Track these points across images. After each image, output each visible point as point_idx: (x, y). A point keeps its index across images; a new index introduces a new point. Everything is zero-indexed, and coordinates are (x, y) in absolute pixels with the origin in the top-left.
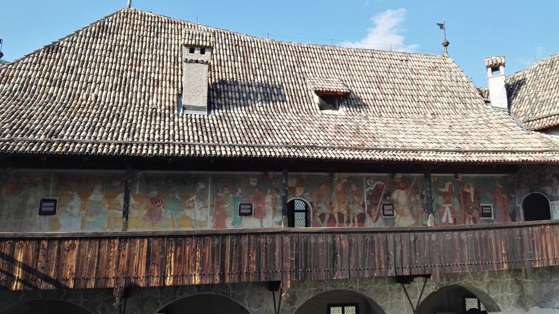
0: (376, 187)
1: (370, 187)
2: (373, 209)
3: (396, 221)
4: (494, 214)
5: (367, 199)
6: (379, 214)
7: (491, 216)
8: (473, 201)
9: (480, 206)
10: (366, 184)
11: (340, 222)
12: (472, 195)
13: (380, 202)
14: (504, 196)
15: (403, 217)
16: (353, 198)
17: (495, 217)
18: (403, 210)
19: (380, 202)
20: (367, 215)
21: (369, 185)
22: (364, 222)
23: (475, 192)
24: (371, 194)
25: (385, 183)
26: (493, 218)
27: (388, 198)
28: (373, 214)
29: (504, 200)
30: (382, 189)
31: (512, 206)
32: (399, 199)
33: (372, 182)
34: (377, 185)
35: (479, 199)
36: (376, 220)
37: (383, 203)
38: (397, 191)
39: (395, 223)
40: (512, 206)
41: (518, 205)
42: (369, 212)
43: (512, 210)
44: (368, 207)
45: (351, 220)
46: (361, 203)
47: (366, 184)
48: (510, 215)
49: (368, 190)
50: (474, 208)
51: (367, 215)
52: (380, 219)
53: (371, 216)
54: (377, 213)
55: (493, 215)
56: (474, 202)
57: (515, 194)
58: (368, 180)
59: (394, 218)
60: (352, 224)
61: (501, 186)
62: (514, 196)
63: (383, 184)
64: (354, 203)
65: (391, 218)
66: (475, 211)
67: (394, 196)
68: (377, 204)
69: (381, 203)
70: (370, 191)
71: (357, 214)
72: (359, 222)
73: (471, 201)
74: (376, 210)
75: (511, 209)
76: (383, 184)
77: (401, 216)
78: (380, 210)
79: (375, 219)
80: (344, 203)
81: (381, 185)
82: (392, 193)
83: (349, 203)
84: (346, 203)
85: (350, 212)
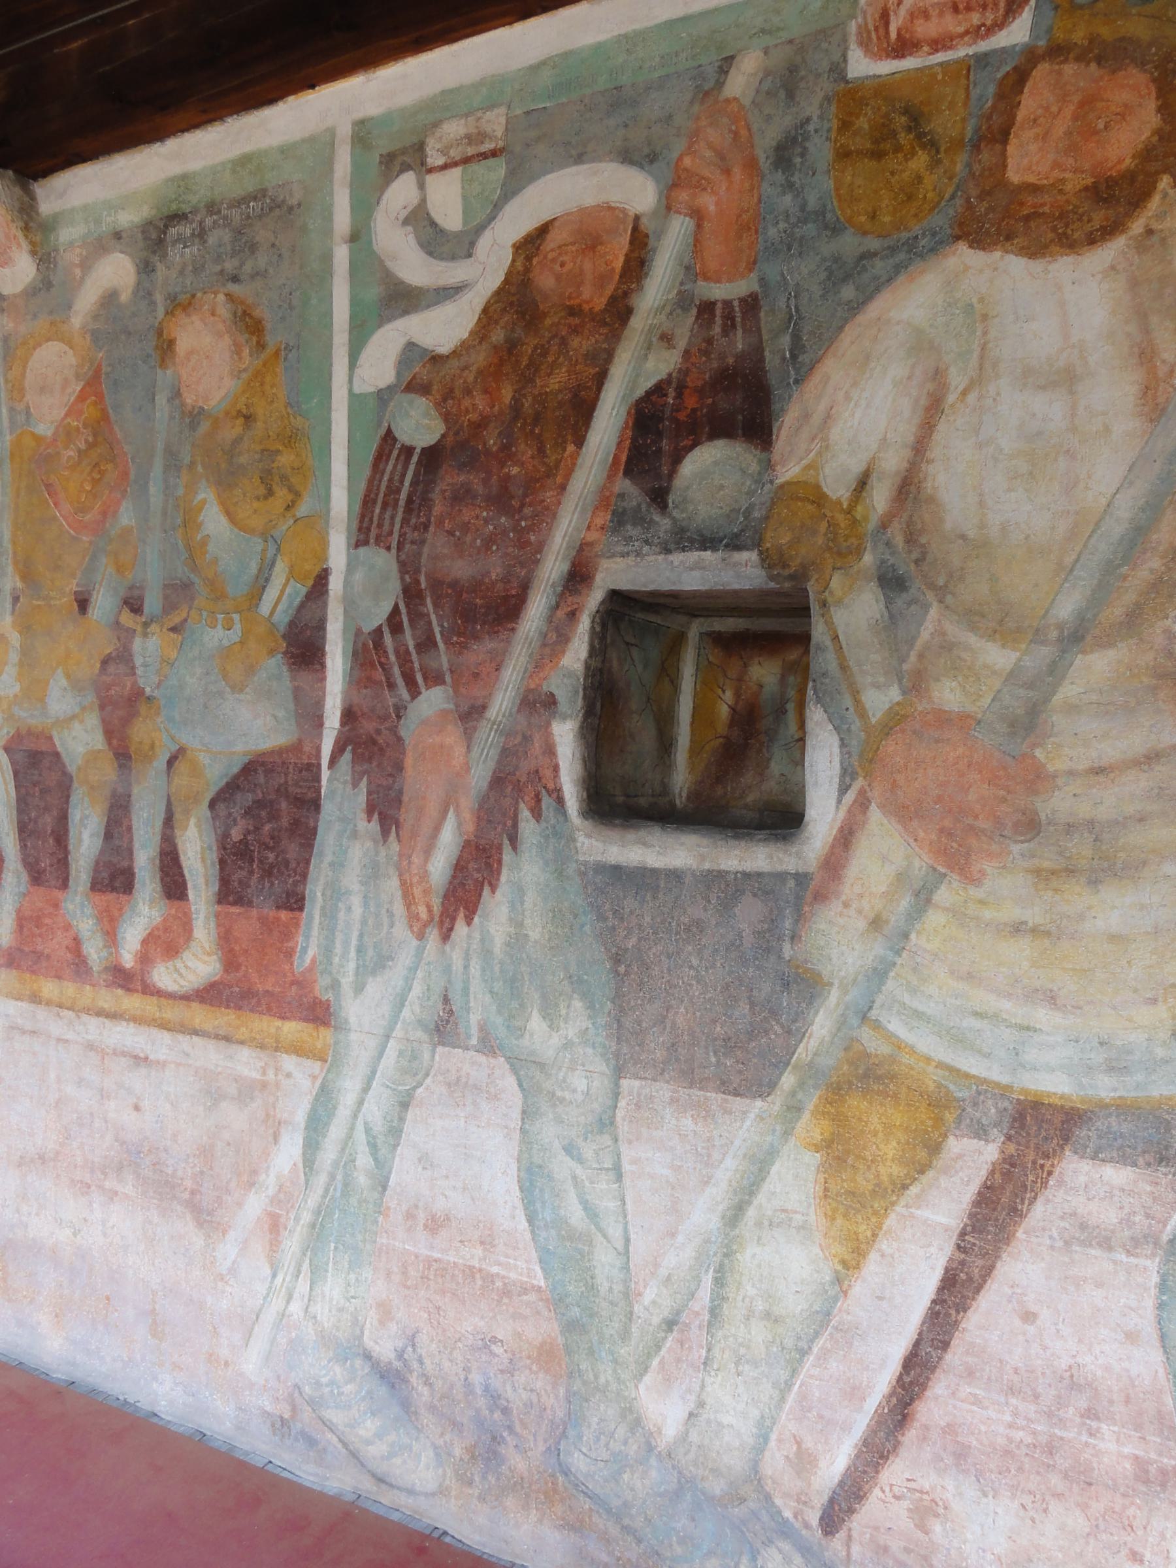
0: (516, 301)
1: (402, 299)
2: (433, 701)
3: (839, 942)
5: (365, 533)
6: (516, 786)
10: (366, 260)
11: (37, 877)
13: (553, 567)
15: (1006, 888)
16: (190, 520)
18: (1028, 722)
19: (553, 567)
20: (341, 796)
21: (414, 267)
22: (295, 902)
24: (420, 426)
25: (676, 185)
27: (710, 472)
28: (421, 782)
30: (619, 312)
32: (953, 482)
33: (447, 198)
34: (531, 246)
36: (465, 892)
37: (619, 572)
38: (914, 303)
39: (804, 984)
42: (372, 743)
44: (367, 654)
45: (144, 858)
46: (280, 598)
47: (366, 260)
49: (379, 365)
51: (341, 796)
52: (525, 872)
53: (386, 810)
54: (480, 775)
58: (402, 192)
59: (810, 891)
60: (145, 912)
63: (637, 192)
64: (184, 594)
65: (729, 889)
67: (850, 417)
68: (506, 609)
69: (578, 576)
70: (423, 374)
71: (216, 772)
72: (229, 893)
74: (470, 714)
76: (637, 192)
77: (956, 848)
78: (537, 704)
79: (439, 866)
80: (83, 604)
81: (590, 229)
82: (801, 363)
83: (134, 605)
84: (103, 604)
85: (140, 732)
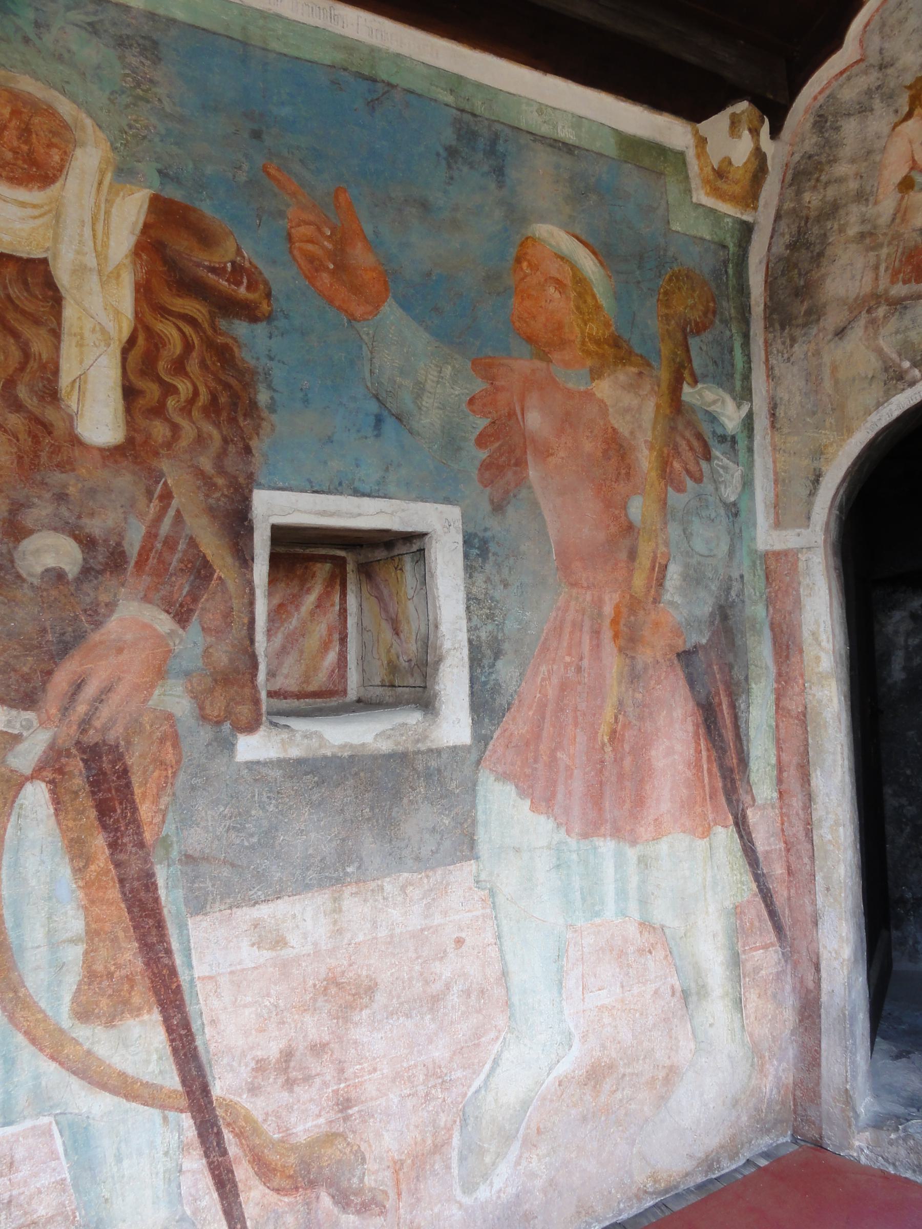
4: (481, 657)
7: (425, 701)
8: (99, 418)
9: (237, 523)
12: (98, 314)
14: (627, 403)
17: (485, 704)
23: (176, 260)
26: (454, 725)
29: (617, 449)
31: (708, 538)
35: (234, 403)
40: (708, 538)
41: (766, 537)
43: (705, 607)
48: (686, 657)
50: (106, 560)
55: (453, 683)
56: (131, 451)
57: (745, 394)
61: (588, 264)
62: (731, 416)
66: (134, 616)
73: (47, 440)
75: (694, 578)
